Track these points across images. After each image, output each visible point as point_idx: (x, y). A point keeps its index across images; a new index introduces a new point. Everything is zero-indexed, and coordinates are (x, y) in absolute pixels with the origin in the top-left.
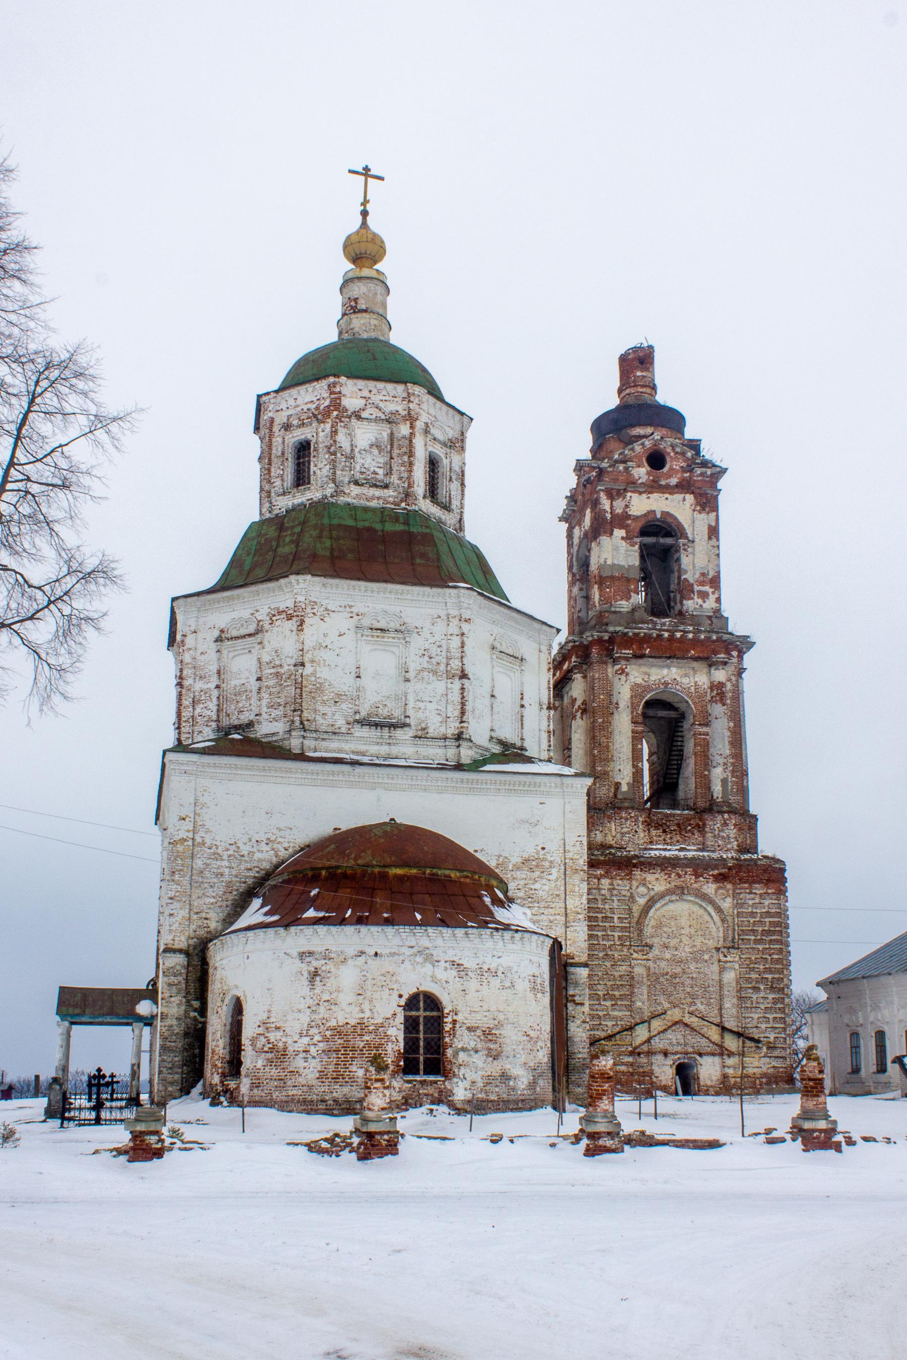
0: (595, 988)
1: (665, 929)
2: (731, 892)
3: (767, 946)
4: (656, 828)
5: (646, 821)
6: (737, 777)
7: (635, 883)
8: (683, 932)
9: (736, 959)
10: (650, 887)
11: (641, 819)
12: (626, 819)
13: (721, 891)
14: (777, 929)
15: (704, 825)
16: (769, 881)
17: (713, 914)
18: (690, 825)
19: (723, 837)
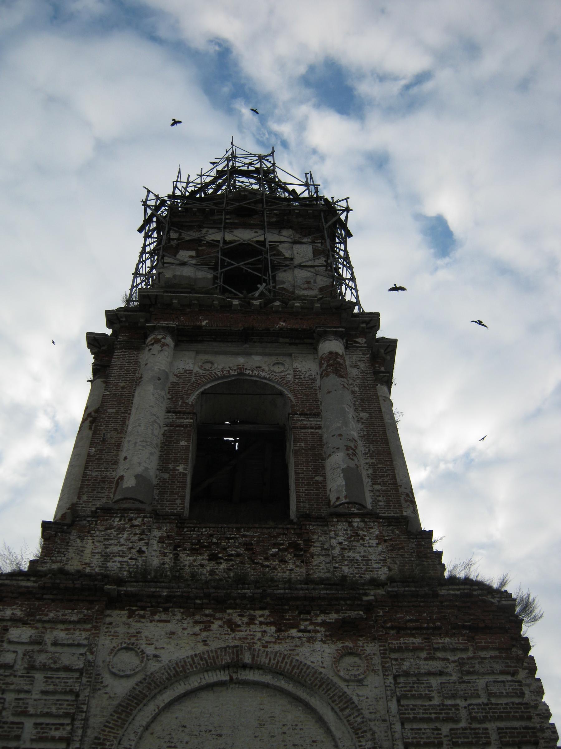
2: (377, 660)
5: (168, 537)
7: (105, 642)
10: (150, 650)
11: (157, 533)
12: (121, 530)
13: (349, 660)
15: (309, 542)
17: (329, 716)
18: (275, 545)
19: (352, 561)
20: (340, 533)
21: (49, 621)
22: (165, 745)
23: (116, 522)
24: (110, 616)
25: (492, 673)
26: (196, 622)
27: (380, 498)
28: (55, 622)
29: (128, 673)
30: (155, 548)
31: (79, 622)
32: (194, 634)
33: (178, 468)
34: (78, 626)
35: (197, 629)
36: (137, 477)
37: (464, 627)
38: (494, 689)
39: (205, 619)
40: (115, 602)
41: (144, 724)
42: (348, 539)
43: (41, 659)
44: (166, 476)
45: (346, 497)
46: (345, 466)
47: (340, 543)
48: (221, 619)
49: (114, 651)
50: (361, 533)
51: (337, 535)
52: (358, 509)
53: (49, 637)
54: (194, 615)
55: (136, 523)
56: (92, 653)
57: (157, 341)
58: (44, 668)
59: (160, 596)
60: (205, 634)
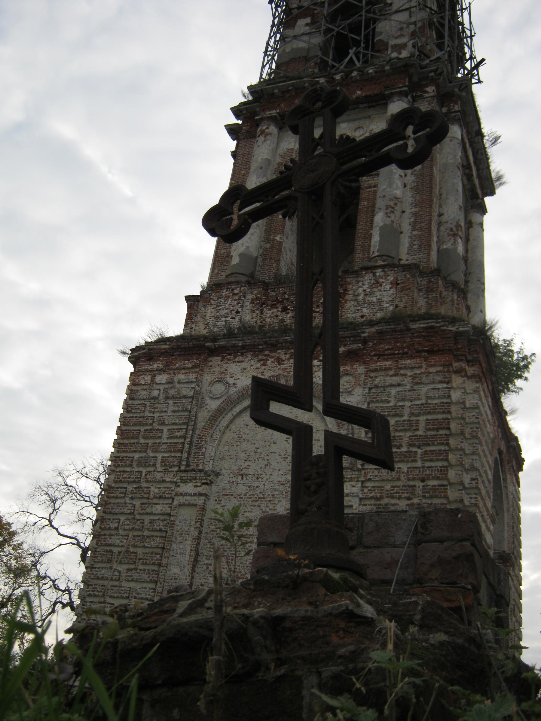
0: (109, 541)
1: (244, 446)
2: (362, 377)
3: (419, 464)
4: (273, 306)
5: (257, 299)
6: (421, 229)
7: (207, 378)
8: (274, 448)
9: (355, 490)
10: (231, 381)
11: (250, 296)
14: (441, 432)
16: (431, 352)
19: (371, 303)
20: (366, 283)
21: (176, 369)
22: (236, 436)
23: (224, 293)
24: (211, 361)
25: (433, 383)
26: (259, 361)
27: (415, 243)
28: (179, 369)
29: (218, 396)
30: (248, 307)
31: (192, 368)
32: (257, 368)
33: (276, 238)
34: (192, 370)
35: (259, 365)
36: (240, 255)
37: (424, 351)
38: (431, 394)
39: (264, 358)
40: (213, 352)
41: (225, 425)
42: (371, 287)
43: (172, 392)
44: (268, 246)
45: (378, 251)
46: (382, 224)
47: (365, 291)
48: (273, 357)
49: (212, 383)
50: (381, 280)
51: (363, 284)
52: (383, 261)
53: (176, 379)
54: (258, 356)
55: (236, 292)
56: (199, 386)
57: (263, 132)
58: (173, 397)
59: (238, 346)
60: (263, 368)
